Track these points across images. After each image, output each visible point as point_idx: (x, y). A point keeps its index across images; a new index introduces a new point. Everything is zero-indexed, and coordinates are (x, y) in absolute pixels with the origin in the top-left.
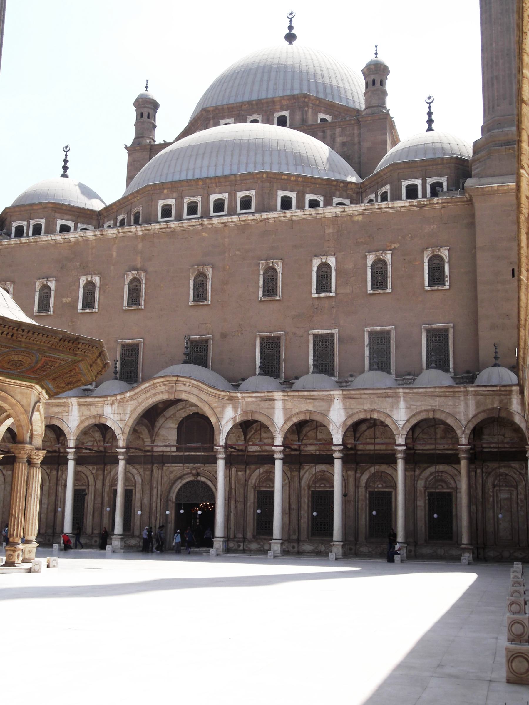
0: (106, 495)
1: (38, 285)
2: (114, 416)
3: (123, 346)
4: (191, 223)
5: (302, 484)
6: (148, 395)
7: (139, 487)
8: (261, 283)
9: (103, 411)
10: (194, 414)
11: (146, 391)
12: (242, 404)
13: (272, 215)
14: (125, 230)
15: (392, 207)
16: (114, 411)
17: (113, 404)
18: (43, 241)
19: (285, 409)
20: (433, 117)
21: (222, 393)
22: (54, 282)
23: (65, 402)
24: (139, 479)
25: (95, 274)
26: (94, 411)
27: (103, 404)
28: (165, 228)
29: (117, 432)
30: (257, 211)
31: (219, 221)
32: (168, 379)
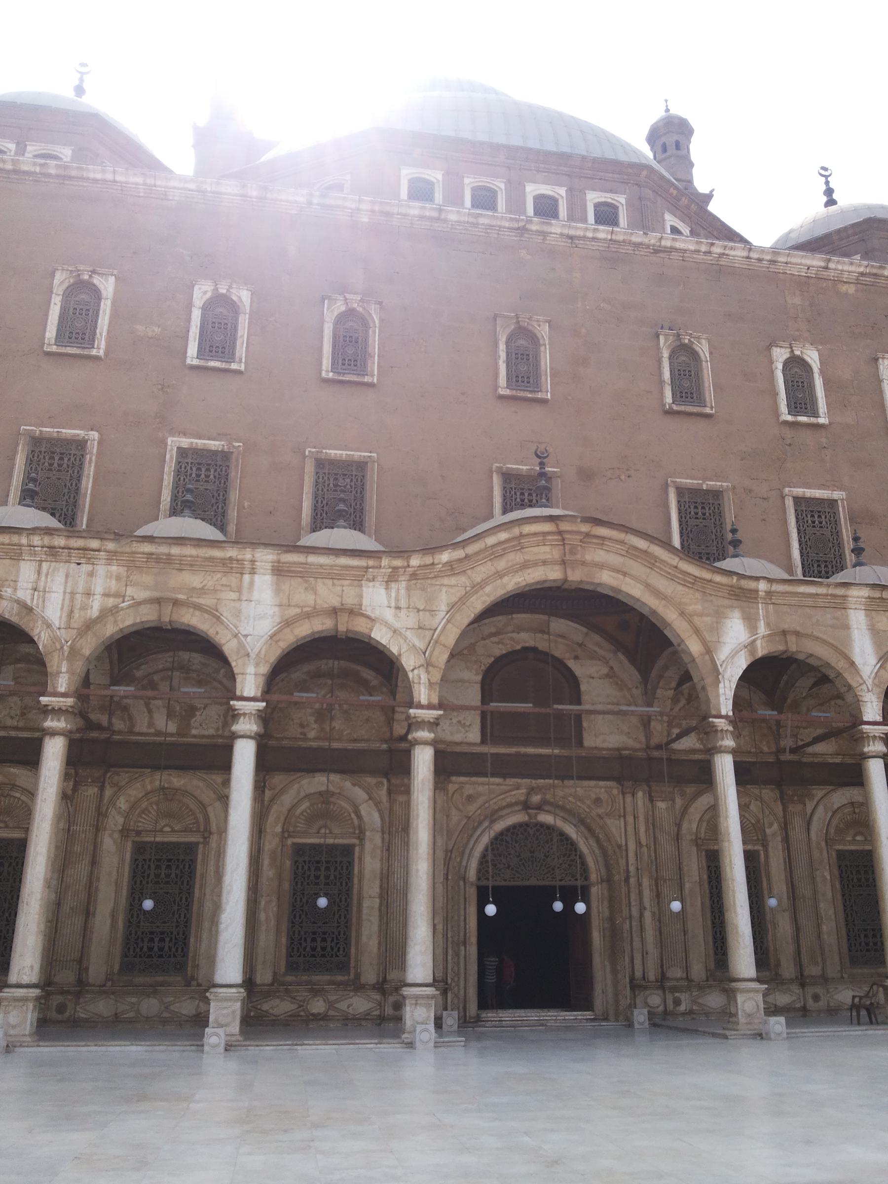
0: (266, 861)
2: (396, 616)
3: (320, 463)
5: (813, 835)
6: (501, 564)
7: (374, 840)
8: (667, 375)
9: (360, 596)
10: (525, 649)
11: (494, 553)
12: (767, 611)
16: (397, 599)
17: (392, 578)
18: (88, 179)
19: (874, 632)
21: (718, 578)
22: (112, 280)
23: (231, 559)
24: (372, 817)
26: (328, 594)
27: (360, 577)
28: (431, 219)
29: (409, 662)
31: (566, 231)
32: (565, 526)
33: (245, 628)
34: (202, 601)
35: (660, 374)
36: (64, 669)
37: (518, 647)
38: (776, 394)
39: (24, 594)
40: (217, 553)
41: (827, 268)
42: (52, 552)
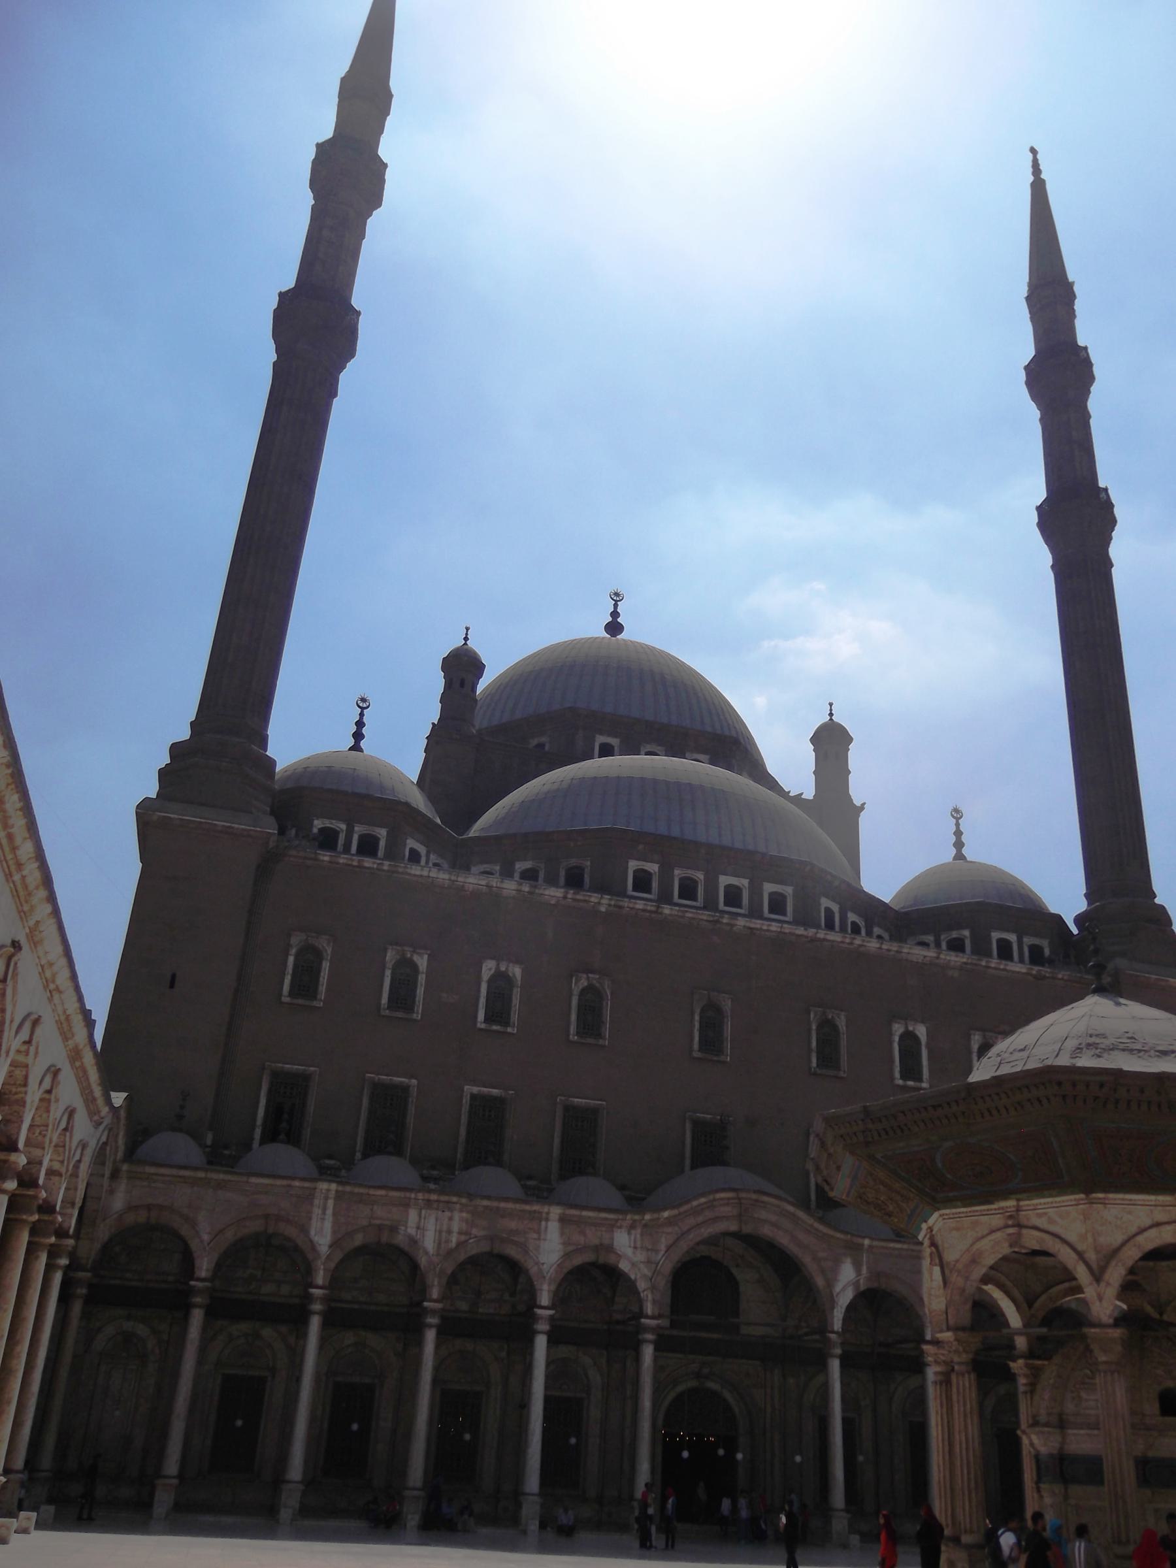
1: (391, 956)
3: (568, 1108)
4: (694, 913)
8: (814, 1044)
9: (612, 1239)
13: (811, 932)
14: (578, 897)
15: (1004, 970)
17: (632, 1227)
18: (410, 874)
20: (964, 838)
21: (838, 1235)
22: (426, 957)
23: (535, 1211)
25: (517, 962)
26: (593, 1237)
27: (612, 1226)
29: (642, 1285)
30: (796, 922)
31: (748, 924)
32: (743, 1195)
33: (543, 1258)
34: (515, 1239)
35: (809, 1043)
36: (436, 1283)
37: (698, 1255)
38: (892, 1061)
39: (412, 1231)
40: (527, 1207)
41: (938, 958)
42: (429, 1204)
